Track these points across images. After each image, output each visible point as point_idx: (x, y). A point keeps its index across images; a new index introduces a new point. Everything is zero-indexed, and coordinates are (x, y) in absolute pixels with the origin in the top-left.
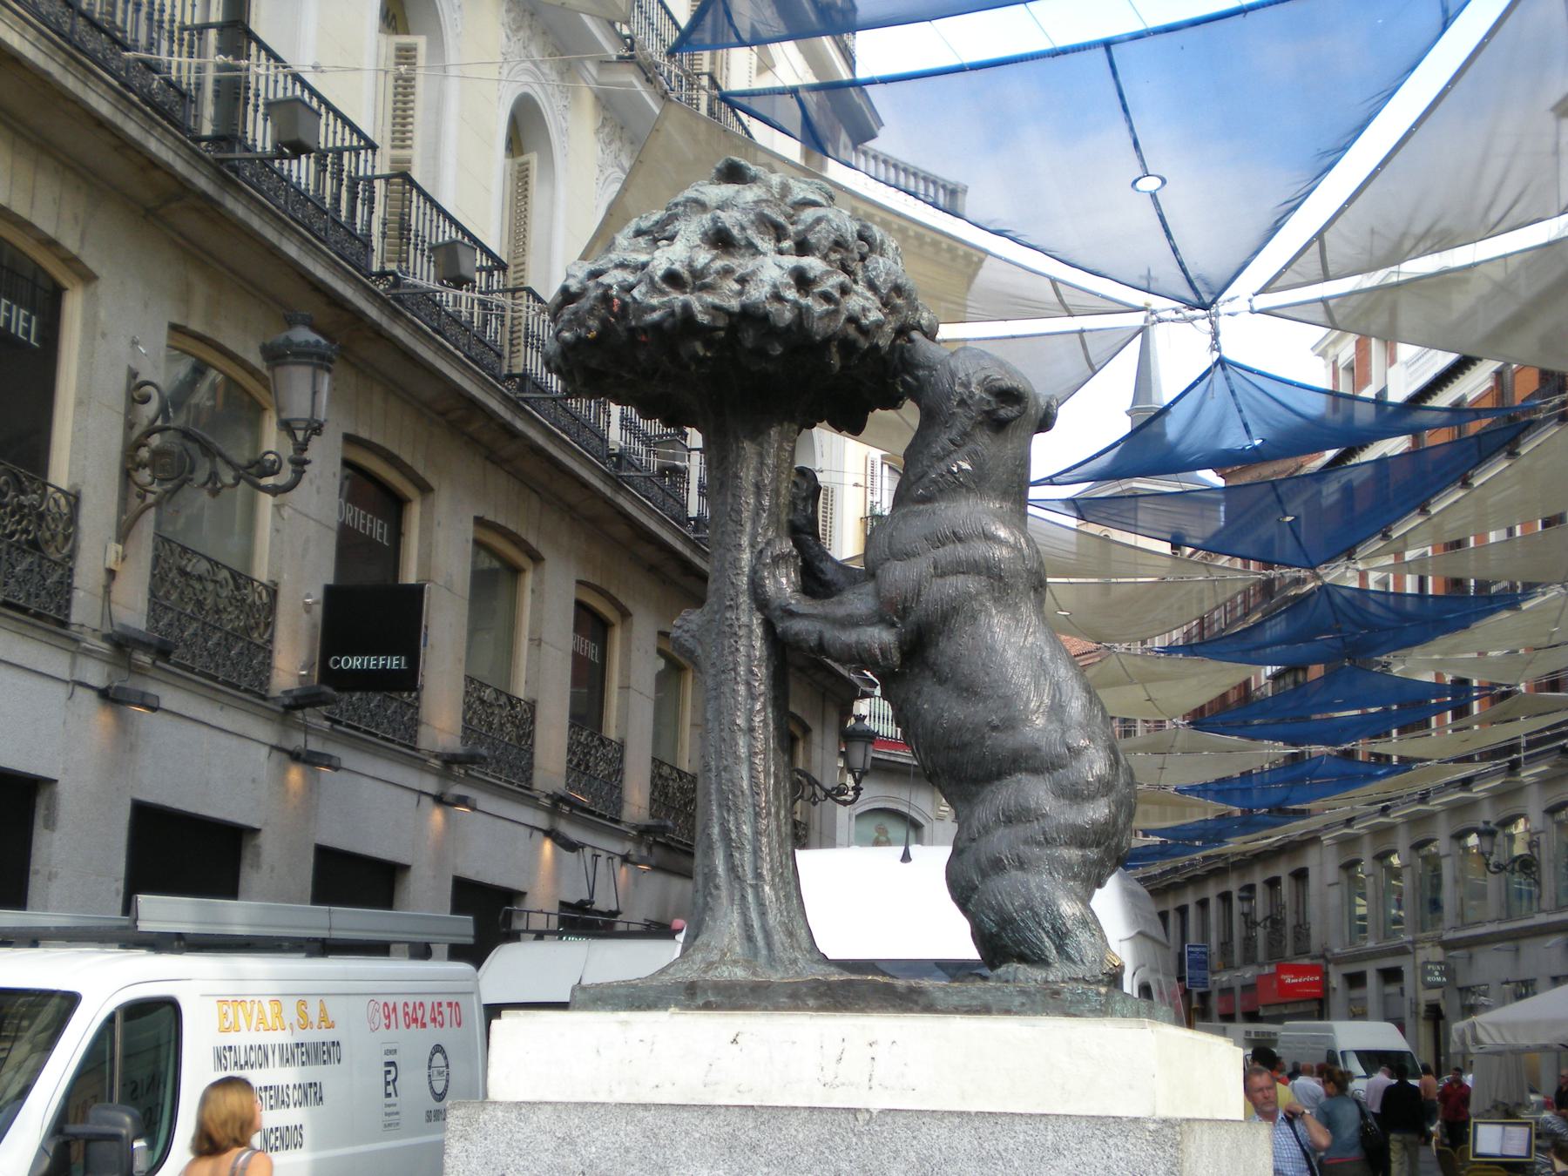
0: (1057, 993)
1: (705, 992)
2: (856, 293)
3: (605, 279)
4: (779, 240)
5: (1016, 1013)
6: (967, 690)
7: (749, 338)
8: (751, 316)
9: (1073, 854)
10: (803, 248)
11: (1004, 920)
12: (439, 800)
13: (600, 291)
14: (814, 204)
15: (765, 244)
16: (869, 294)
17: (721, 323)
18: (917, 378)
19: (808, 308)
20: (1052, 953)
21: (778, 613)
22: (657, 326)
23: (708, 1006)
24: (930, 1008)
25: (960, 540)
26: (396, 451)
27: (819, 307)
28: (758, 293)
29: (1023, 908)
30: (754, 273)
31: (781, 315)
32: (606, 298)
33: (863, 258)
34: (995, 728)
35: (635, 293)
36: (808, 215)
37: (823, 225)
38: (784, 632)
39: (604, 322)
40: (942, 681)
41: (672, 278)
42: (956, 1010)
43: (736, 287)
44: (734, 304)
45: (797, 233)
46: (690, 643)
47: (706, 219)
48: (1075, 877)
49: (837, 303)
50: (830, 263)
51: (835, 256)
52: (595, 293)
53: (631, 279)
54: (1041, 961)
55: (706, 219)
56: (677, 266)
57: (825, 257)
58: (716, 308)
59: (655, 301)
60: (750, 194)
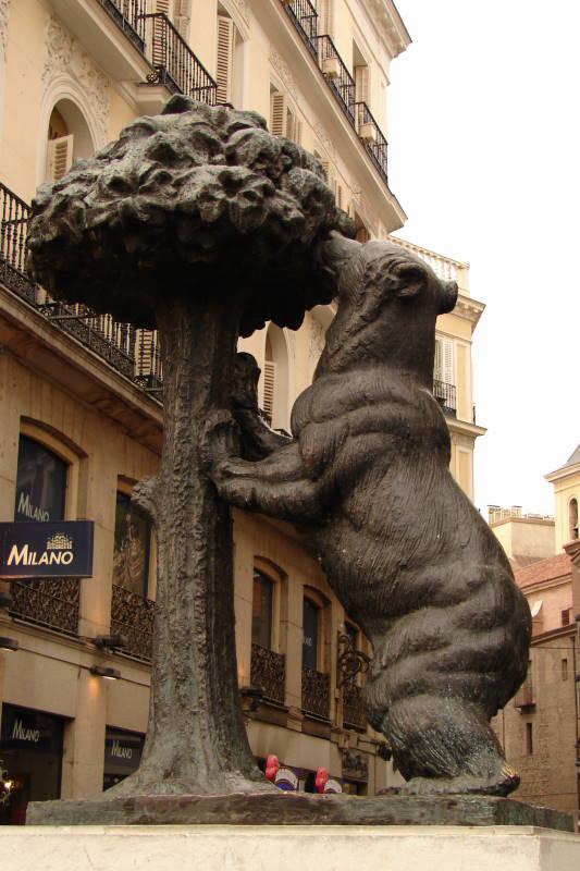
0: (453, 803)
1: (141, 807)
2: (279, 196)
3: (64, 192)
4: (212, 154)
5: (417, 823)
6: (378, 534)
7: (185, 233)
8: (186, 215)
9: (475, 677)
10: (232, 159)
11: (410, 738)
12: (95, 672)
13: (61, 200)
14: (246, 126)
15: (202, 158)
16: (291, 197)
17: (159, 220)
18: (335, 269)
19: (234, 204)
20: (453, 769)
21: (219, 475)
22: (104, 224)
23: (144, 821)
24: (340, 820)
25: (372, 403)
26: (60, 429)
27: (245, 204)
28: (190, 194)
29: (429, 727)
30: (187, 177)
31: (209, 211)
33: (287, 169)
34: (404, 567)
35: (88, 200)
36: (239, 134)
37: (251, 141)
38: (224, 491)
40: (357, 527)
41: (117, 184)
42: (362, 822)
43: (172, 190)
44: (171, 203)
45: (230, 148)
46: (147, 505)
47: (150, 141)
48: (475, 699)
49: (260, 201)
50: (256, 171)
51: (259, 166)
52: (55, 202)
53: (85, 189)
55: (150, 141)
56: (122, 175)
57: (251, 167)
58: (152, 207)
59: (103, 205)
60: (187, 119)
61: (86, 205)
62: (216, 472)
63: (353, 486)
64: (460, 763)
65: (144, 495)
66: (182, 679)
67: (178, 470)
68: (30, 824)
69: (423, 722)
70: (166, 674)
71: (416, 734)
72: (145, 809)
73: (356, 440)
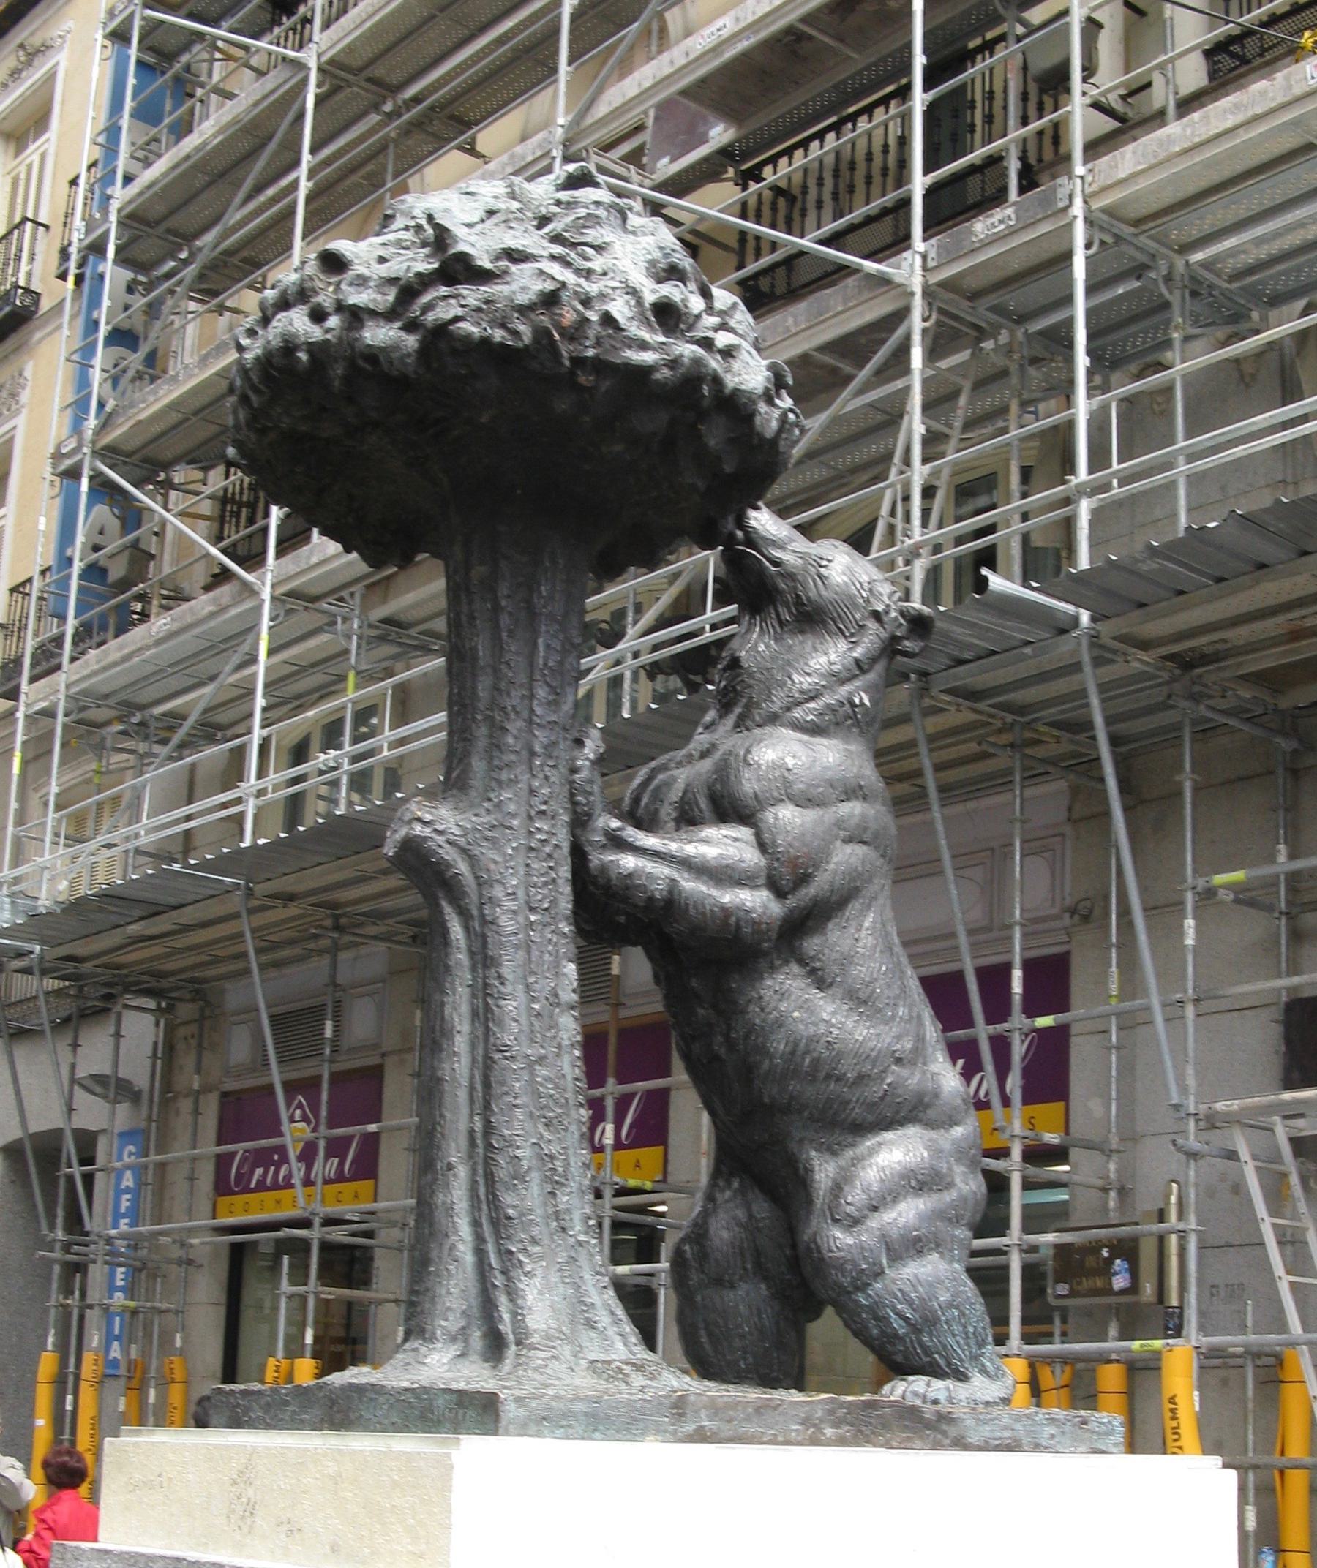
6: (865, 1003)
11: (926, 1319)
13: (549, 286)
18: (776, 563)
22: (644, 372)
23: (701, 1436)
29: (950, 1305)
32: (550, 300)
38: (604, 868)
39: (542, 335)
40: (820, 981)
42: (984, 1447)
46: (448, 854)
54: (962, 1377)
59: (645, 335)
61: (608, 320)
62: (594, 830)
63: (829, 919)
64: (975, 1358)
65: (441, 833)
66: (554, 1183)
67: (543, 812)
68: (507, 1433)
69: (944, 1297)
70: (530, 1169)
71: (934, 1312)
72: (703, 1414)
73: (849, 849)
